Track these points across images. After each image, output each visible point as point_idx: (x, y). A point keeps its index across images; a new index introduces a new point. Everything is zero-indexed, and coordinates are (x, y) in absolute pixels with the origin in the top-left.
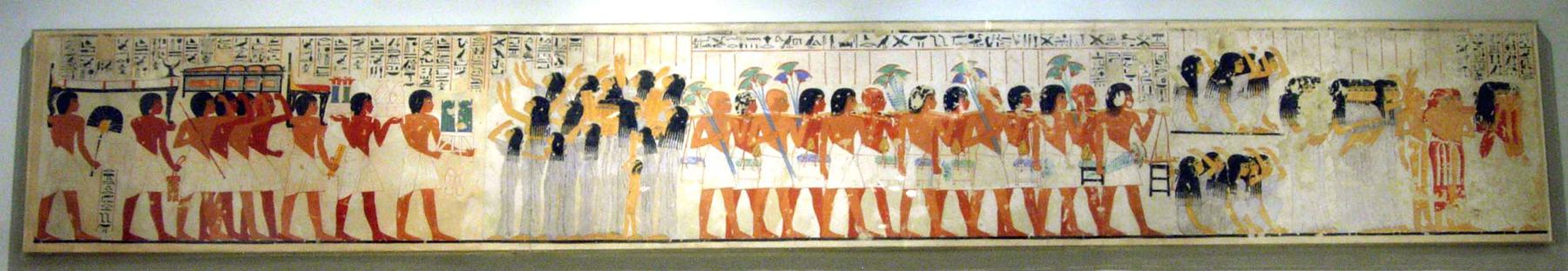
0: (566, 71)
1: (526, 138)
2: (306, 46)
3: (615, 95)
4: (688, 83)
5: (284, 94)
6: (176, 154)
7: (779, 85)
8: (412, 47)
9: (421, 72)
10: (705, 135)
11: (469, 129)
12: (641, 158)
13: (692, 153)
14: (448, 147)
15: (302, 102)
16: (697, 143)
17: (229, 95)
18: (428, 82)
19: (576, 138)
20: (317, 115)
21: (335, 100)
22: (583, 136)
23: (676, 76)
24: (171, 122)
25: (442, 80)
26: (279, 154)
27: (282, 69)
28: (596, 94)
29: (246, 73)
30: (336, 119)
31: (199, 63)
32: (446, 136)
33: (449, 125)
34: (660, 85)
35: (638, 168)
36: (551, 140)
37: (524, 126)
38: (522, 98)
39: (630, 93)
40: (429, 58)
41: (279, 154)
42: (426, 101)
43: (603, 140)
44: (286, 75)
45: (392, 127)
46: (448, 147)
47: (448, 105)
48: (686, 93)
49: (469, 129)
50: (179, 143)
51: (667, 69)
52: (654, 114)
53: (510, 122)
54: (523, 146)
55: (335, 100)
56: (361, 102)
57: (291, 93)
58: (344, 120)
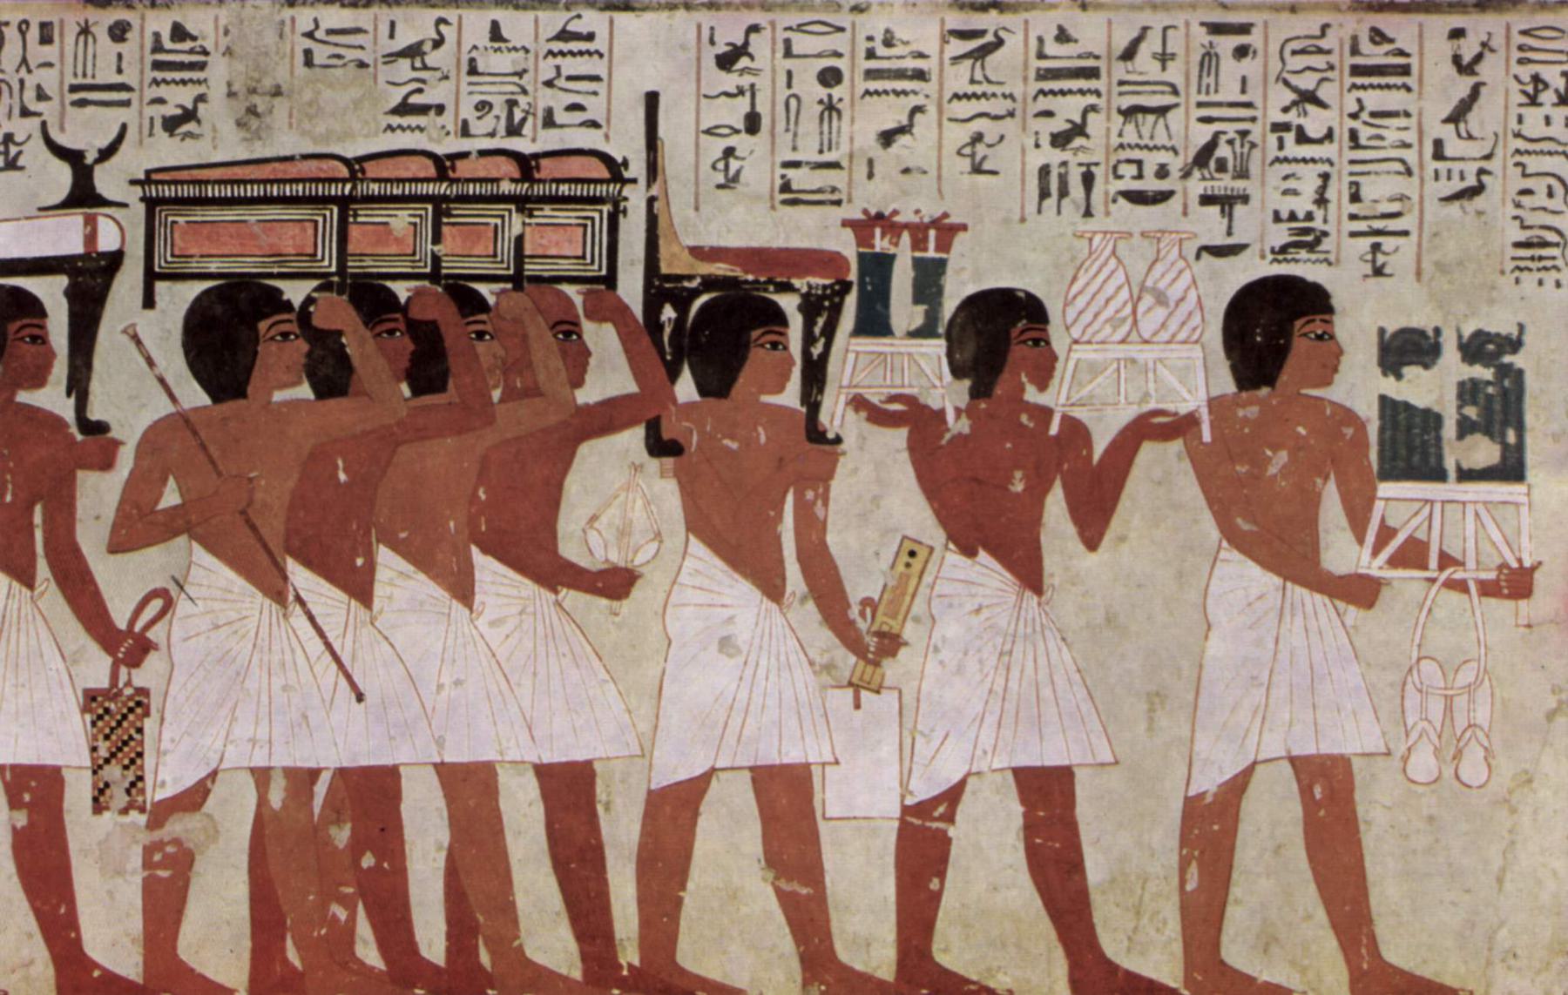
2: (726, 62)
5: (631, 288)
6: (123, 583)
8: (1231, 70)
9: (1271, 194)
11: (1511, 469)
14: (1412, 555)
15: (718, 325)
17: (370, 297)
18: (1308, 240)
20: (790, 396)
21: (874, 323)
24: (100, 428)
25: (1377, 232)
26: (615, 583)
27: (616, 170)
29: (445, 189)
30: (878, 417)
31: (219, 142)
33: (1411, 446)
40: (1315, 121)
41: (615, 583)
42: (1302, 334)
44: (635, 199)
45: (1148, 452)
47: (1406, 349)
49: (1511, 469)
50: (136, 528)
55: (874, 323)
56: (999, 332)
57: (660, 288)
58: (916, 419)
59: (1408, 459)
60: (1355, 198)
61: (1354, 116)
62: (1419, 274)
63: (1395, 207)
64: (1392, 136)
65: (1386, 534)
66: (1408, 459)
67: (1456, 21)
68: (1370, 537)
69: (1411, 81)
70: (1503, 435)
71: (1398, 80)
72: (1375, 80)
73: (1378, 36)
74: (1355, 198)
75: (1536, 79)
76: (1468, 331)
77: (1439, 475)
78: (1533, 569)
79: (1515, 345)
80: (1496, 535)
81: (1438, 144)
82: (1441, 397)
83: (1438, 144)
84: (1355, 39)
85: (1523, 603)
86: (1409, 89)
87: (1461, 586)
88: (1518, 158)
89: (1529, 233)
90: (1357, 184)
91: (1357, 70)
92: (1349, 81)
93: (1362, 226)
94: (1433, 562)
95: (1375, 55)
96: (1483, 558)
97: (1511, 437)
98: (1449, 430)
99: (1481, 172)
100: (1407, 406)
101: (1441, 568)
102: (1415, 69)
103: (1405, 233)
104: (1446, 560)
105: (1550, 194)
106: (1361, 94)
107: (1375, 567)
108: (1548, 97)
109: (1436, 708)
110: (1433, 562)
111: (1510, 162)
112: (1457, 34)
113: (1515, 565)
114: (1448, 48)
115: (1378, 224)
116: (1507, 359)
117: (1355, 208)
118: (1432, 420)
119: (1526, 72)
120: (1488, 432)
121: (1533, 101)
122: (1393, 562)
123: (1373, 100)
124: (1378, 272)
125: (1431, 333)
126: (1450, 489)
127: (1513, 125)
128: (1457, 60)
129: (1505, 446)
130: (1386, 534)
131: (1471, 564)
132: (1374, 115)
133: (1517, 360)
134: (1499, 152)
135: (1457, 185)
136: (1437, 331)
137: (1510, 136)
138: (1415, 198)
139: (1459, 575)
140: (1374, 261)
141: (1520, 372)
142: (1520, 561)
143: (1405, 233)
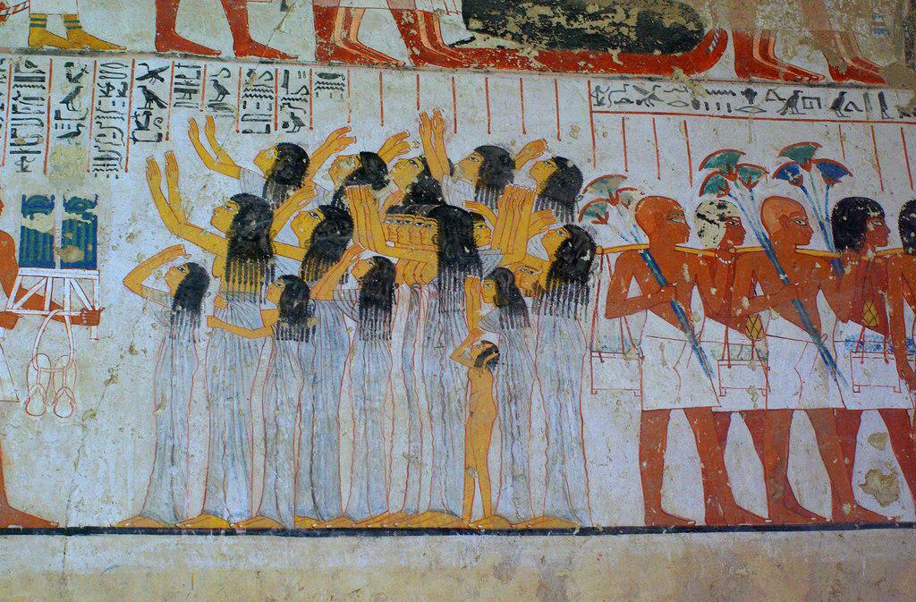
0: (308, 140)
1: (214, 286)
3: (425, 196)
4: (589, 175)
7: (783, 188)
10: (634, 290)
11: (90, 263)
12: (492, 337)
13: (609, 329)
14: (36, 302)
16: (619, 306)
19: (339, 286)
22: (353, 285)
23: (560, 161)
28: (382, 195)
32: (29, 277)
34: (526, 179)
35: (488, 357)
36: (276, 292)
37: (211, 257)
38: (210, 198)
39: (459, 193)
43: (403, 291)
46: (36, 302)
48: (586, 198)
49: (90, 263)
51: (540, 145)
52: (521, 239)
53: (178, 249)
54: (207, 304)
59: (35, 257)
60: (14, 136)
61: (15, 99)
62: (45, 171)
63: (35, 140)
64: (34, 108)
65: (22, 292)
66: (35, 257)
67: (70, 59)
68: (13, 294)
69: (46, 84)
70: (86, 247)
71: (39, 84)
72: (27, 84)
73: (29, 64)
74: (14, 136)
75: (108, 85)
76: (68, 199)
77: (51, 265)
78: (100, 311)
79: (93, 205)
80: (81, 295)
81: (58, 112)
82: (53, 230)
83: (58, 112)
84: (18, 65)
85: (94, 328)
86: (44, 88)
87: (62, 319)
88: (98, 120)
89: (102, 154)
90: (15, 130)
91: (17, 79)
92: (13, 83)
93: (17, 149)
94: (47, 305)
95: (26, 72)
96: (73, 305)
97: (90, 248)
98: (58, 243)
99: (79, 125)
100: (36, 232)
101: (51, 310)
102: (47, 80)
103: (39, 152)
104: (53, 306)
105: (114, 137)
106: (19, 89)
107: (15, 308)
108: (114, 93)
109: (44, 377)
110: (47, 305)
111: (94, 121)
112: (69, 65)
113: (91, 309)
114: (65, 71)
115: (24, 148)
116: (88, 211)
117: (13, 141)
118: (49, 238)
119: (103, 82)
120: (78, 245)
121: (107, 95)
122: (25, 306)
123: (25, 92)
124: (24, 170)
125: (49, 198)
126: (57, 272)
127: (96, 104)
128: (69, 76)
129: (86, 252)
130: (22, 292)
131: (67, 308)
132: (24, 99)
133: (94, 211)
134: (88, 117)
135: (66, 131)
136: (53, 197)
137: (94, 109)
138: (45, 137)
139: (63, 314)
140: (22, 165)
141: (96, 217)
142: (93, 307)
143: (39, 152)
